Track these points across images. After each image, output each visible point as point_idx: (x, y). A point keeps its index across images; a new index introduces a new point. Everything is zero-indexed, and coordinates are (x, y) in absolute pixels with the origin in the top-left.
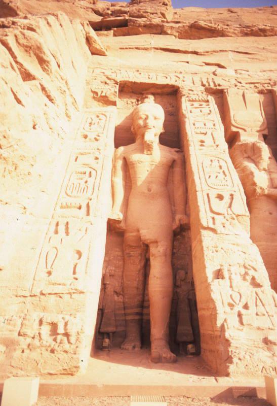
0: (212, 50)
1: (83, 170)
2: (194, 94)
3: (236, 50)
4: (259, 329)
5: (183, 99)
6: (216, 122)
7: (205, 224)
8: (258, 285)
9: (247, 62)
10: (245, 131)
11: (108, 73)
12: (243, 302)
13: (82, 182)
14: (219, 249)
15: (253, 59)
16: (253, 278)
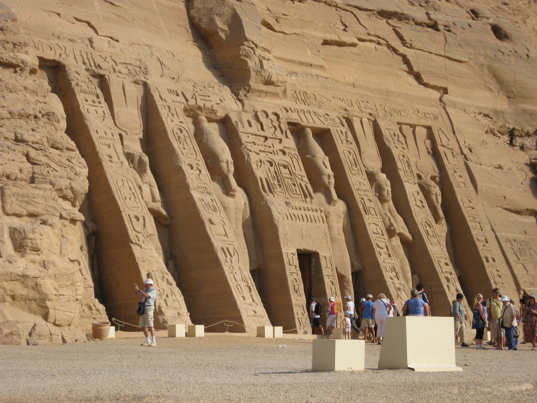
5: (77, 90)
7: (134, 241)
8: (171, 284)
10: (127, 134)
12: (166, 294)
14: (145, 260)
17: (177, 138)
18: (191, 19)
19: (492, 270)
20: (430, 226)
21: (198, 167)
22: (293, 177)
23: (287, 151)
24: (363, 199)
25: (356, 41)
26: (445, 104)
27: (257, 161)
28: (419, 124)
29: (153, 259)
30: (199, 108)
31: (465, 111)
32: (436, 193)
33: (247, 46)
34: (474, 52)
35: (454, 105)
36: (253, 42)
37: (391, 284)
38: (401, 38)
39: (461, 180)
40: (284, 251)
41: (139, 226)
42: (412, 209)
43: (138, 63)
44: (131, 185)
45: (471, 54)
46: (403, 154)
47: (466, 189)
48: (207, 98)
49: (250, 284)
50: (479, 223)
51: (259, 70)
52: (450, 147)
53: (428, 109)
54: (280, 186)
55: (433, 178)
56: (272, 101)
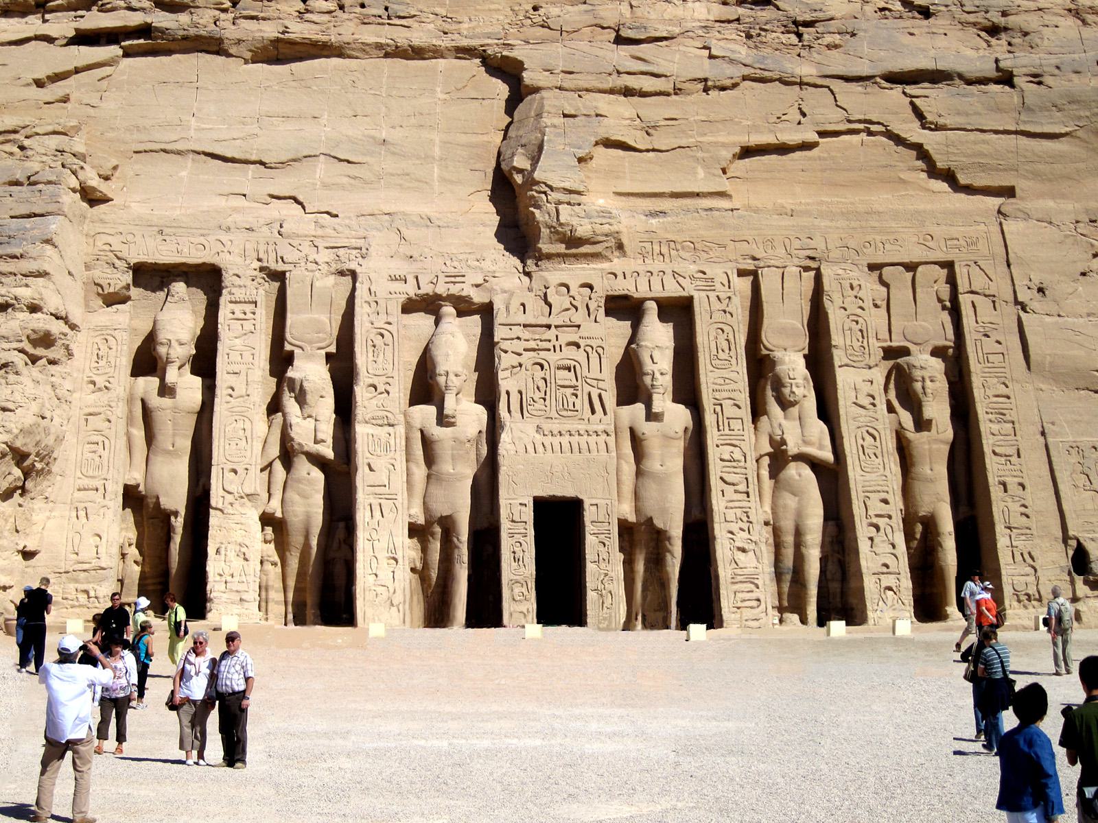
0: (290, 157)
1: (95, 438)
2: (240, 286)
3: (332, 154)
4: (237, 591)
5: (223, 300)
6: (256, 352)
8: (246, 560)
9: (343, 188)
11: (116, 243)
13: (97, 459)
15: (355, 178)
16: (244, 554)
17: (371, 349)
18: (499, 154)
19: (1010, 504)
20: (875, 438)
21: (388, 388)
22: (579, 384)
23: (582, 343)
24: (721, 405)
25: (815, 137)
26: (1005, 215)
27: (513, 367)
29: (239, 526)
30: (438, 297)
31: (1051, 223)
32: (923, 378)
33: (537, 192)
34: (1088, 114)
36: (545, 183)
37: (727, 543)
38: (919, 114)
39: (998, 348)
40: (503, 502)
41: (233, 483)
42: (842, 411)
43: (360, 243)
44: (248, 425)
45: (1080, 118)
46: (856, 318)
48: (458, 279)
49: (399, 556)
50: (1013, 423)
51: (554, 224)
53: (955, 231)
54: (545, 400)
55: (937, 352)
56: (592, 266)
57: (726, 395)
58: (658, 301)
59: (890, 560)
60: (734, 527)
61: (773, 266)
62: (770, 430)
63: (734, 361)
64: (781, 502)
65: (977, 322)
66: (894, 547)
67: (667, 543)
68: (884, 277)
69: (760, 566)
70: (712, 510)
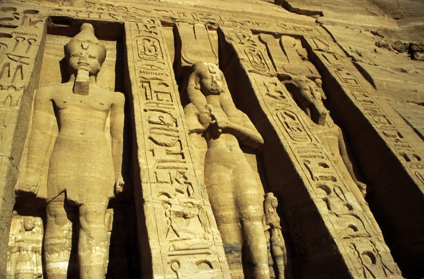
19: (418, 170)
28: (285, 33)
32: (310, 88)
35: (333, 24)
37: (159, 206)
42: (259, 98)
46: (253, 49)
47: (358, 85)
50: (384, 117)
52: (331, 50)
57: (154, 76)
58: (94, 23)
59: (355, 222)
60: (170, 189)
61: (186, 22)
62: (197, 111)
63: (160, 57)
64: (215, 175)
65: (330, 63)
66: (350, 208)
67: (82, 220)
68: (262, 38)
69: (210, 236)
70: (139, 169)
